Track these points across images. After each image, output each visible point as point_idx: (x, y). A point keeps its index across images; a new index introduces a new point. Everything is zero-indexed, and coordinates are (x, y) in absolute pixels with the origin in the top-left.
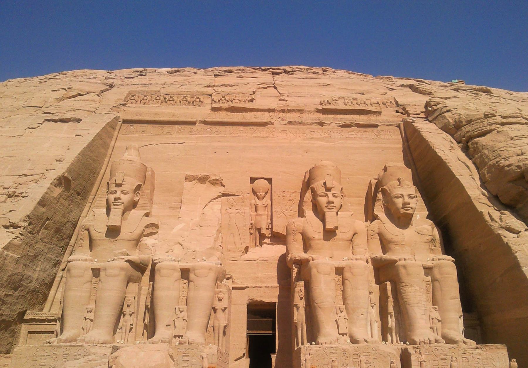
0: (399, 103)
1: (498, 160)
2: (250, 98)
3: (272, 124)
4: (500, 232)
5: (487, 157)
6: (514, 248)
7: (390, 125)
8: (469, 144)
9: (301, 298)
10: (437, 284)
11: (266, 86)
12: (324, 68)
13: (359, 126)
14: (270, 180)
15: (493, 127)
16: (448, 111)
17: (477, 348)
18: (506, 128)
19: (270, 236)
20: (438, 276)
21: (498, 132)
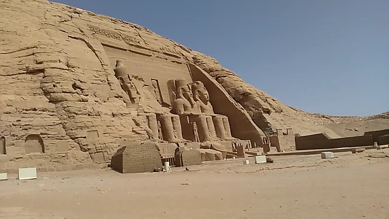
0: (184, 55)
1: (235, 87)
2: (138, 41)
3: (152, 56)
4: (240, 109)
5: (229, 85)
6: (246, 114)
7: (184, 64)
8: (219, 78)
9: (196, 128)
10: (225, 123)
11: (136, 35)
12: (146, 28)
13: (177, 62)
14: (157, 81)
15: (227, 75)
16: (204, 63)
17: (245, 141)
18: (230, 76)
19: (161, 103)
20: (225, 121)
21: (230, 77)
